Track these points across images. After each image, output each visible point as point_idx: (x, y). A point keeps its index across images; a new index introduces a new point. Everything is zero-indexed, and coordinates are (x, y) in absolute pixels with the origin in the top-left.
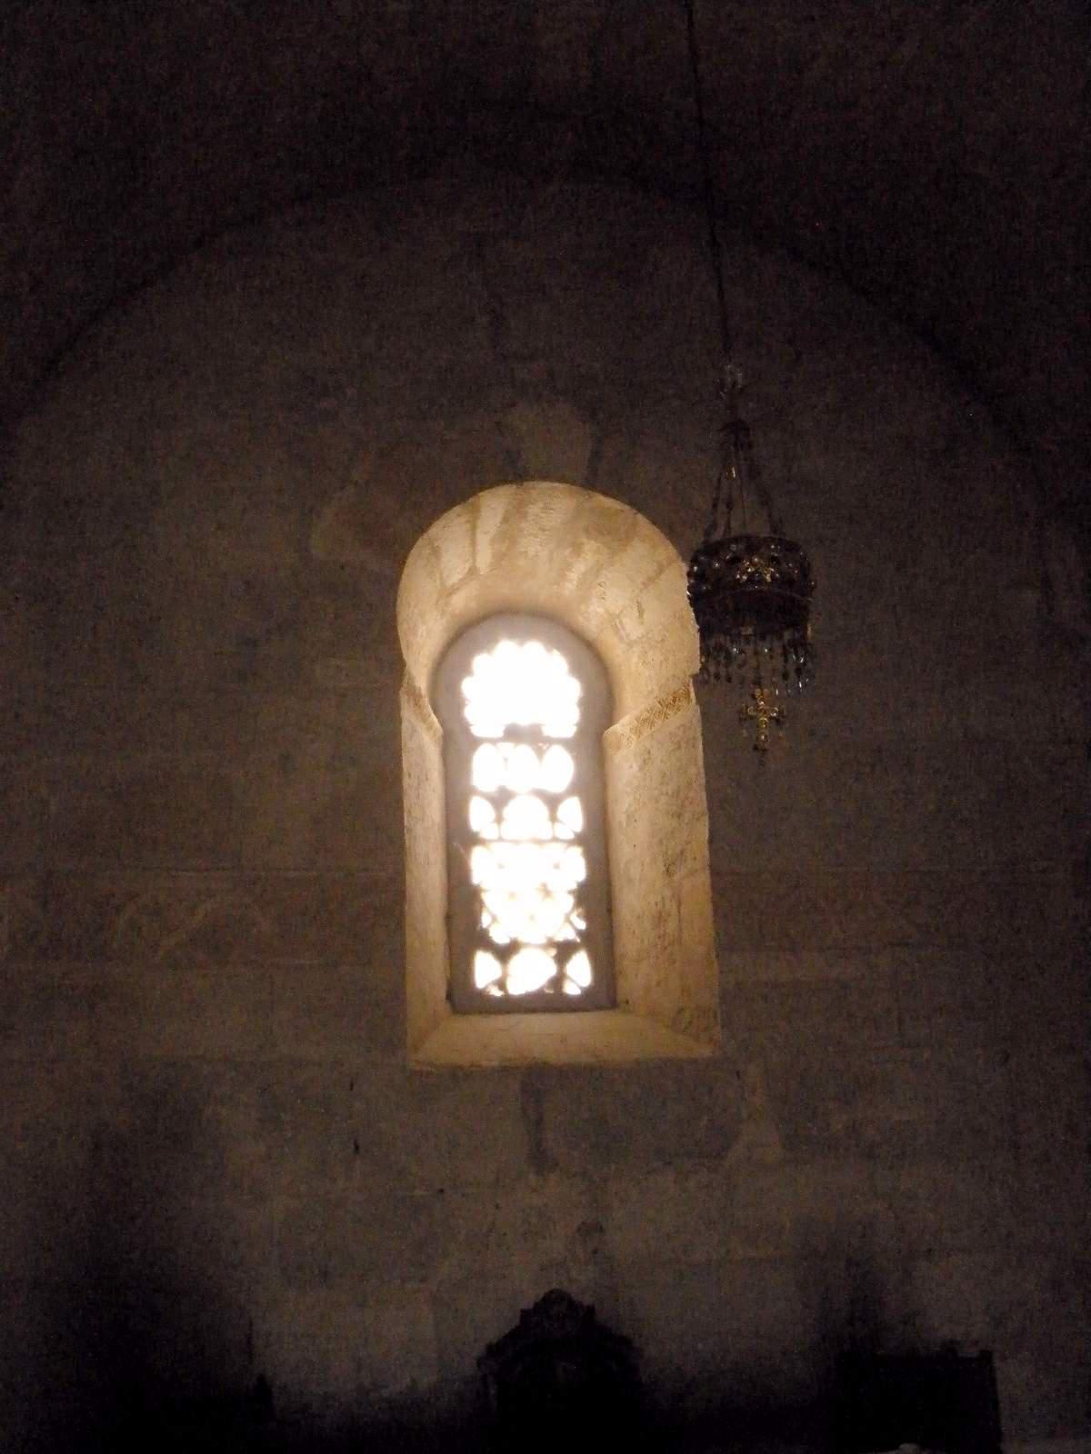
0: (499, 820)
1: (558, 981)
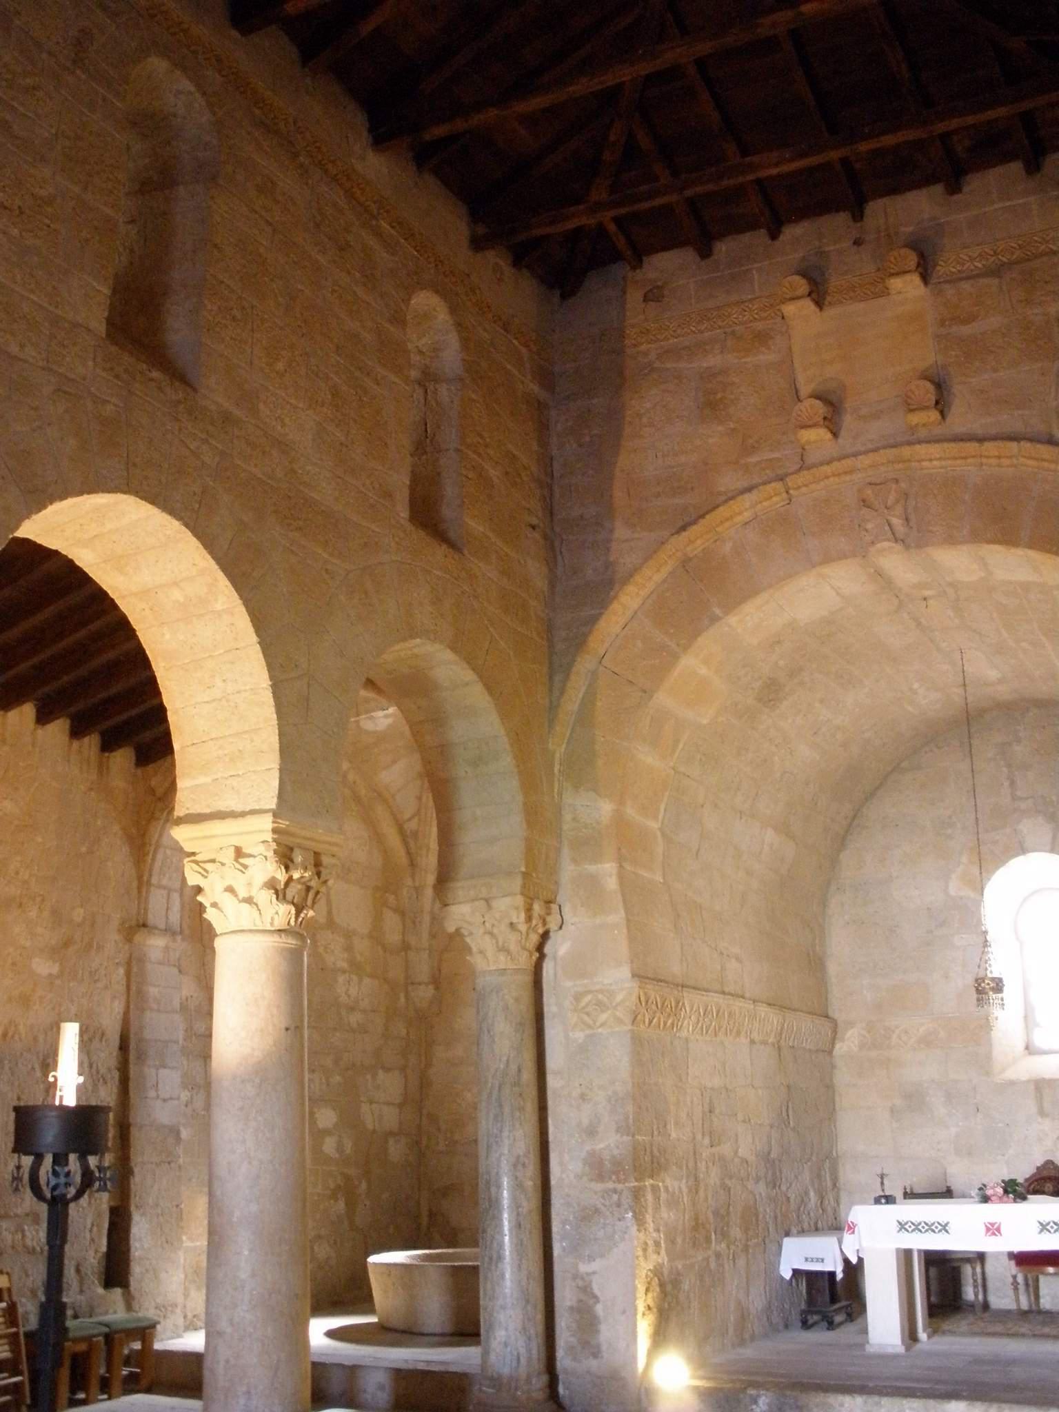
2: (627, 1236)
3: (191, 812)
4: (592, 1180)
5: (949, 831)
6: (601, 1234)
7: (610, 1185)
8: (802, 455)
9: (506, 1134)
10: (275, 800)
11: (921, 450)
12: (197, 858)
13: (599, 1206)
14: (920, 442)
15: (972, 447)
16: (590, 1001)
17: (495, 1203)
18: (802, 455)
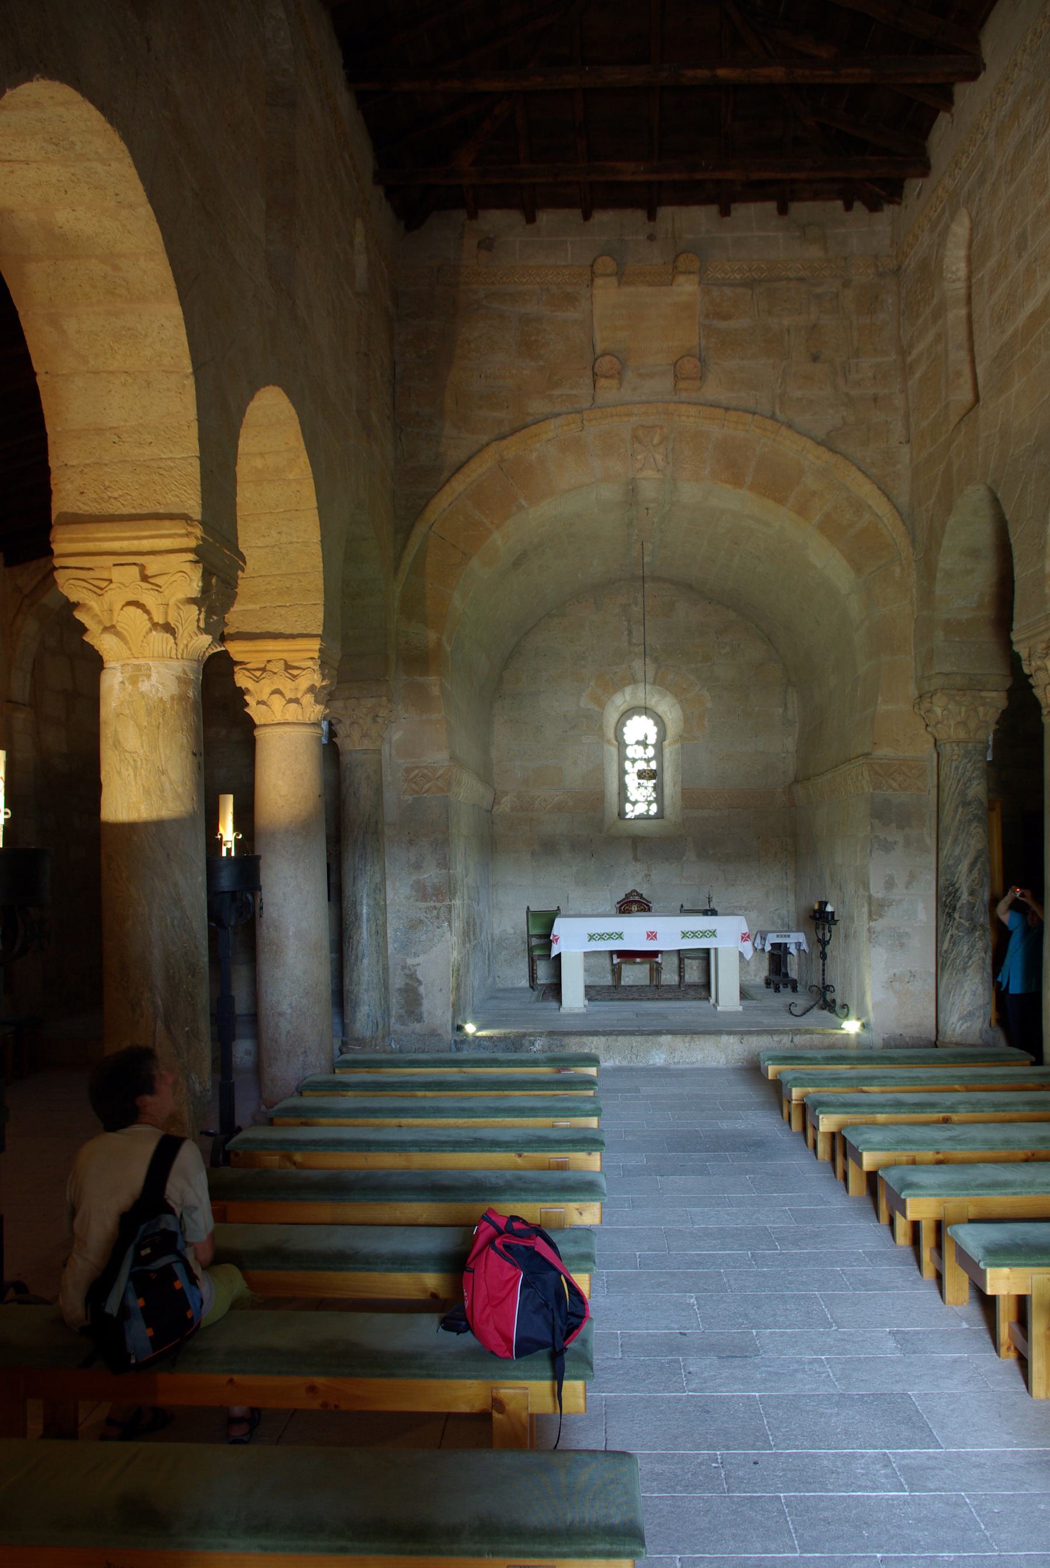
0: (633, 767)
1: (648, 811)
2: (443, 939)
3: (240, 630)
4: (417, 901)
5: (583, 663)
6: (423, 938)
7: (432, 904)
8: (594, 395)
9: (368, 868)
10: (322, 628)
11: (683, 408)
12: (248, 666)
13: (423, 918)
14: (683, 403)
15: (720, 412)
16: (418, 774)
17: (358, 917)
18: (594, 395)
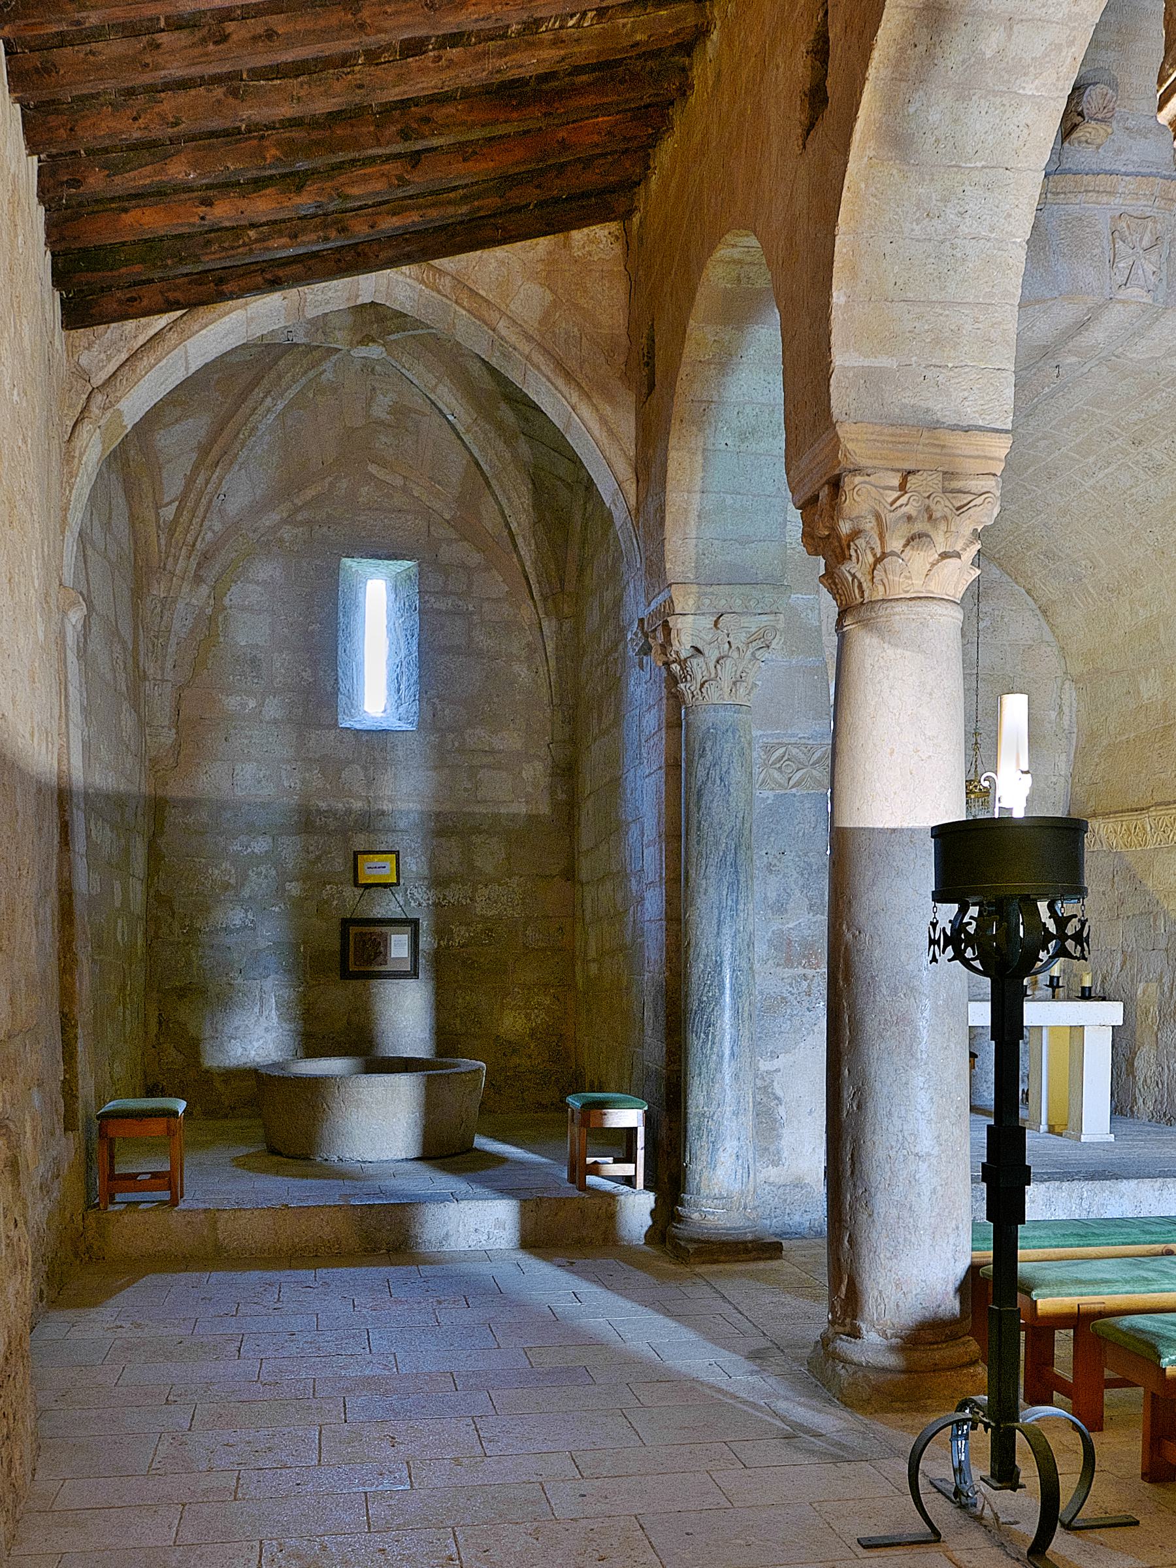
4: (778, 965)
6: (786, 1026)
7: (800, 971)
